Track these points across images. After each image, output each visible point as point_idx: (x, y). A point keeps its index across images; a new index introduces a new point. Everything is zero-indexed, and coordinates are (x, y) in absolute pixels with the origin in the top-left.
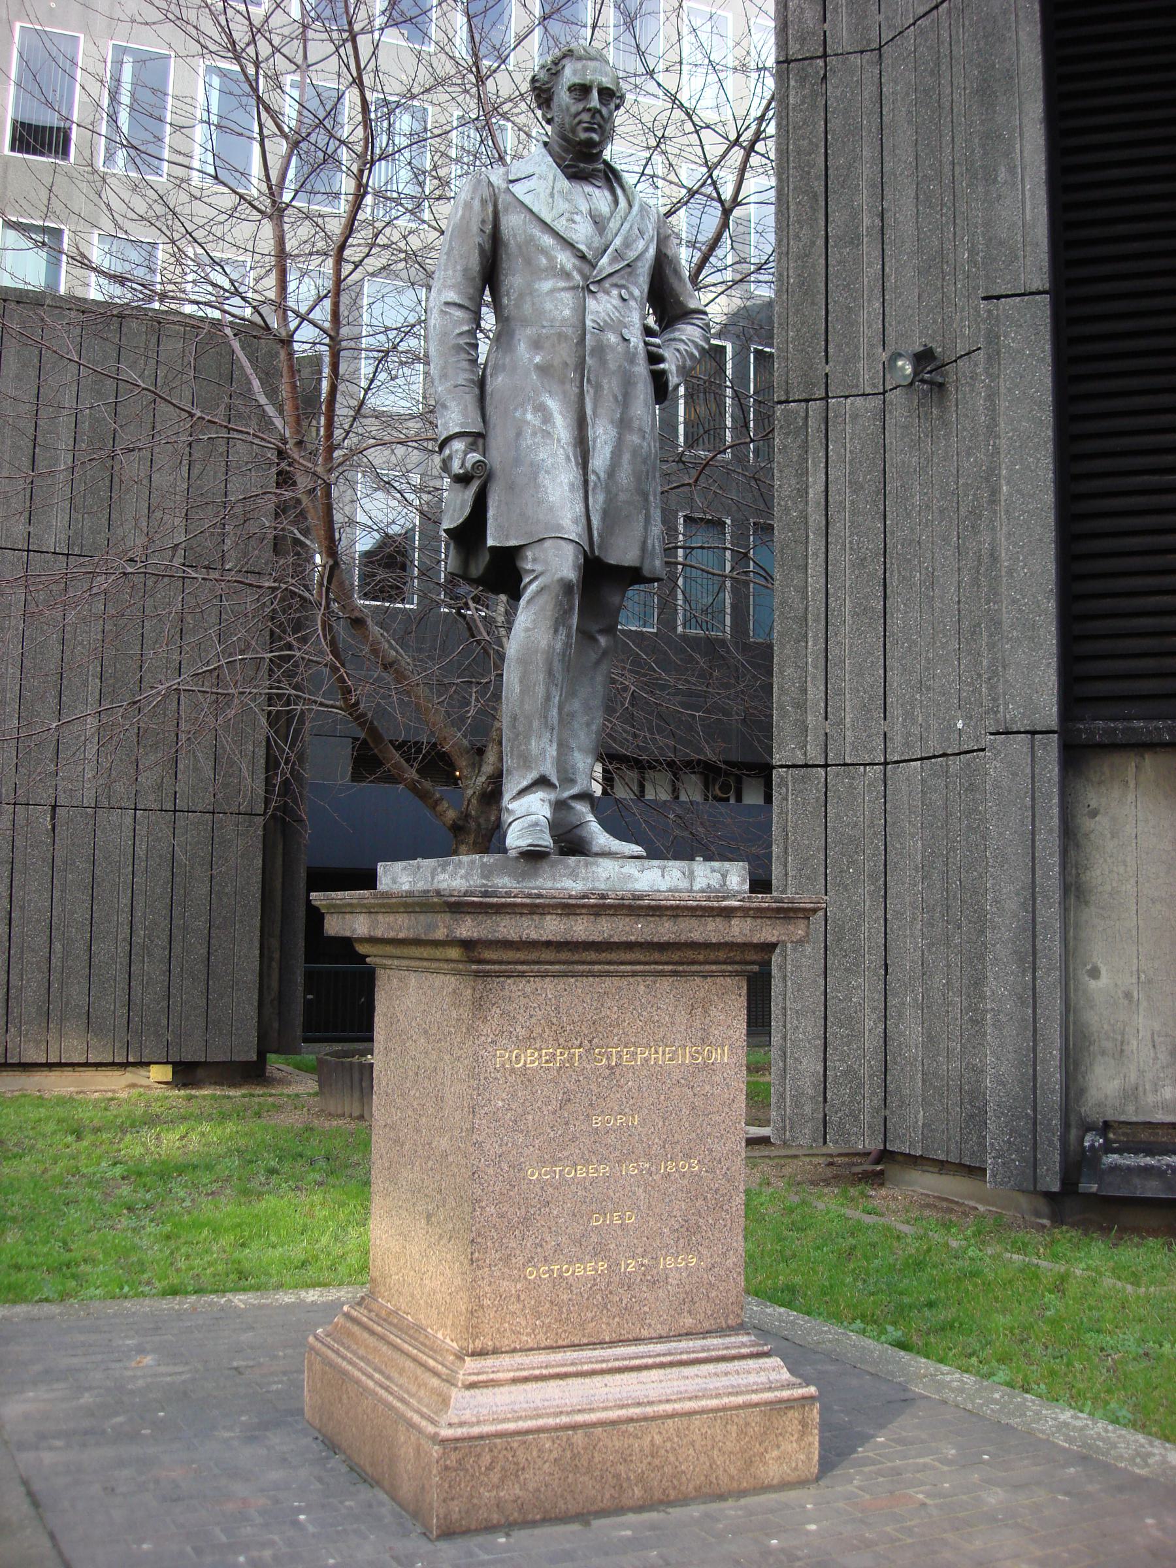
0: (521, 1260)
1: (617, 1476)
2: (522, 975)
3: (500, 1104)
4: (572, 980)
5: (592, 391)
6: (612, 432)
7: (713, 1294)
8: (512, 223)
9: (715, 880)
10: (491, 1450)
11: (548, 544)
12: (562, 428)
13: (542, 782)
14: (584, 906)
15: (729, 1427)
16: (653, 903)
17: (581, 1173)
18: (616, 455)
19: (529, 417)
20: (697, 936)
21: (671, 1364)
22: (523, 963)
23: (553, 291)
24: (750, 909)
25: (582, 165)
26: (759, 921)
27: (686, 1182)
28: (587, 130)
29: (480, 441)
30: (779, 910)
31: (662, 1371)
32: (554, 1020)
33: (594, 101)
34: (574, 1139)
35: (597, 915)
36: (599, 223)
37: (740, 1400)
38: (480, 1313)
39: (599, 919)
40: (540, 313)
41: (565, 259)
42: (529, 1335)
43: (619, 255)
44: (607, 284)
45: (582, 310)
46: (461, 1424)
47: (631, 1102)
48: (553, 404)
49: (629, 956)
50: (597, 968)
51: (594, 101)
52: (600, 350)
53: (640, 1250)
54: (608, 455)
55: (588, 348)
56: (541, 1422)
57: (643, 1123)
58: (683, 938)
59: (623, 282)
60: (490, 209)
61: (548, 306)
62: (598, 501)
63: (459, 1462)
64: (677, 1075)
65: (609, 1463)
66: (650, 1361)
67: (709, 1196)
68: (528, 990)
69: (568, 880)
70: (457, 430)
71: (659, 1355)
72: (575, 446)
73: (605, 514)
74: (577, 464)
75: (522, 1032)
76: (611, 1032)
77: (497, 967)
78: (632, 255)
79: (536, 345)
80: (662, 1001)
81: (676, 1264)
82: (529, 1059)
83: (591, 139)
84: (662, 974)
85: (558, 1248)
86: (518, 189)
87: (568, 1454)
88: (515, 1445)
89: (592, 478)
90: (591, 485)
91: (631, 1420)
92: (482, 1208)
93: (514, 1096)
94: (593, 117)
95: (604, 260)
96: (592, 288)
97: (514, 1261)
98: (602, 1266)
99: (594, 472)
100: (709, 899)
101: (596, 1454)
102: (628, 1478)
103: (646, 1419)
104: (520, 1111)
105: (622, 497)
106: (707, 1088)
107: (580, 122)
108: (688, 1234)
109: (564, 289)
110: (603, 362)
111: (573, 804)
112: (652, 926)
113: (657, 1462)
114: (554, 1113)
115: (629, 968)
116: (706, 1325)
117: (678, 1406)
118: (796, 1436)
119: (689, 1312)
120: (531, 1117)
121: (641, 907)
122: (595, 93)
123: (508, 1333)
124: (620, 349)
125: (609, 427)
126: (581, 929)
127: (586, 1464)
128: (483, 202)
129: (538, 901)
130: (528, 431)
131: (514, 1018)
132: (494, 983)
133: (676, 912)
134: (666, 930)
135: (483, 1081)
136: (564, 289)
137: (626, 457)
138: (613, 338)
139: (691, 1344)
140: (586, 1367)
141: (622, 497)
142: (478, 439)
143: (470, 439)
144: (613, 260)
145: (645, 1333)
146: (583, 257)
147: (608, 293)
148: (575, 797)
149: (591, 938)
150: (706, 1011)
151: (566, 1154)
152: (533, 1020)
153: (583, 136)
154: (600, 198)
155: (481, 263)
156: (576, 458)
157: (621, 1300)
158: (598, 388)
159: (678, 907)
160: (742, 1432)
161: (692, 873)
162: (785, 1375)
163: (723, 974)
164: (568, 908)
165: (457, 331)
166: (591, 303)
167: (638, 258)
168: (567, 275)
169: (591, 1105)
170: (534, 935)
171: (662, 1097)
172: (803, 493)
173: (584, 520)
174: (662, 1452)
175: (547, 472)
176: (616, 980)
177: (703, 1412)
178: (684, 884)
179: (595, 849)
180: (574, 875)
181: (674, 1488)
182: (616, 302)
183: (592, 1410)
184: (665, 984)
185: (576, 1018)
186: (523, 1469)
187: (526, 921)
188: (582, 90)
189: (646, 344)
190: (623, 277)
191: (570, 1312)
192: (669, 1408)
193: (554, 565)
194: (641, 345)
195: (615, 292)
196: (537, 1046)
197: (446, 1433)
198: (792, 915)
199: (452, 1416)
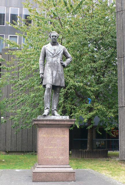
6: (56, 72)
8: (46, 51)
12: (50, 72)
13: (47, 108)
20: (61, 123)
21: (59, 168)
33: (54, 37)
36: (55, 50)
37: (66, 171)
40: (49, 60)
41: (51, 54)
45: (52, 60)
48: (49, 70)
49: (55, 126)
51: (54, 37)
52: (54, 64)
62: (54, 79)
69: (52, 117)
73: (55, 80)
78: (58, 53)
79: (48, 63)
80: (59, 130)
81: (61, 158)
82: (44, 136)
95: (55, 54)
105: (57, 79)
108: (62, 154)
110: (55, 65)
126: (48, 123)
134: (57, 123)
138: (56, 62)
141: (57, 79)
142: (43, 74)
144: (56, 54)
154: (55, 47)
158: (54, 68)
164: (47, 120)
166: (53, 59)
167: (59, 53)
172: (121, 70)
180: (49, 117)
182: (56, 58)
184: (59, 129)
187: (42, 122)
188: (53, 36)
193: (48, 86)
194: (60, 62)
197: (33, 171)
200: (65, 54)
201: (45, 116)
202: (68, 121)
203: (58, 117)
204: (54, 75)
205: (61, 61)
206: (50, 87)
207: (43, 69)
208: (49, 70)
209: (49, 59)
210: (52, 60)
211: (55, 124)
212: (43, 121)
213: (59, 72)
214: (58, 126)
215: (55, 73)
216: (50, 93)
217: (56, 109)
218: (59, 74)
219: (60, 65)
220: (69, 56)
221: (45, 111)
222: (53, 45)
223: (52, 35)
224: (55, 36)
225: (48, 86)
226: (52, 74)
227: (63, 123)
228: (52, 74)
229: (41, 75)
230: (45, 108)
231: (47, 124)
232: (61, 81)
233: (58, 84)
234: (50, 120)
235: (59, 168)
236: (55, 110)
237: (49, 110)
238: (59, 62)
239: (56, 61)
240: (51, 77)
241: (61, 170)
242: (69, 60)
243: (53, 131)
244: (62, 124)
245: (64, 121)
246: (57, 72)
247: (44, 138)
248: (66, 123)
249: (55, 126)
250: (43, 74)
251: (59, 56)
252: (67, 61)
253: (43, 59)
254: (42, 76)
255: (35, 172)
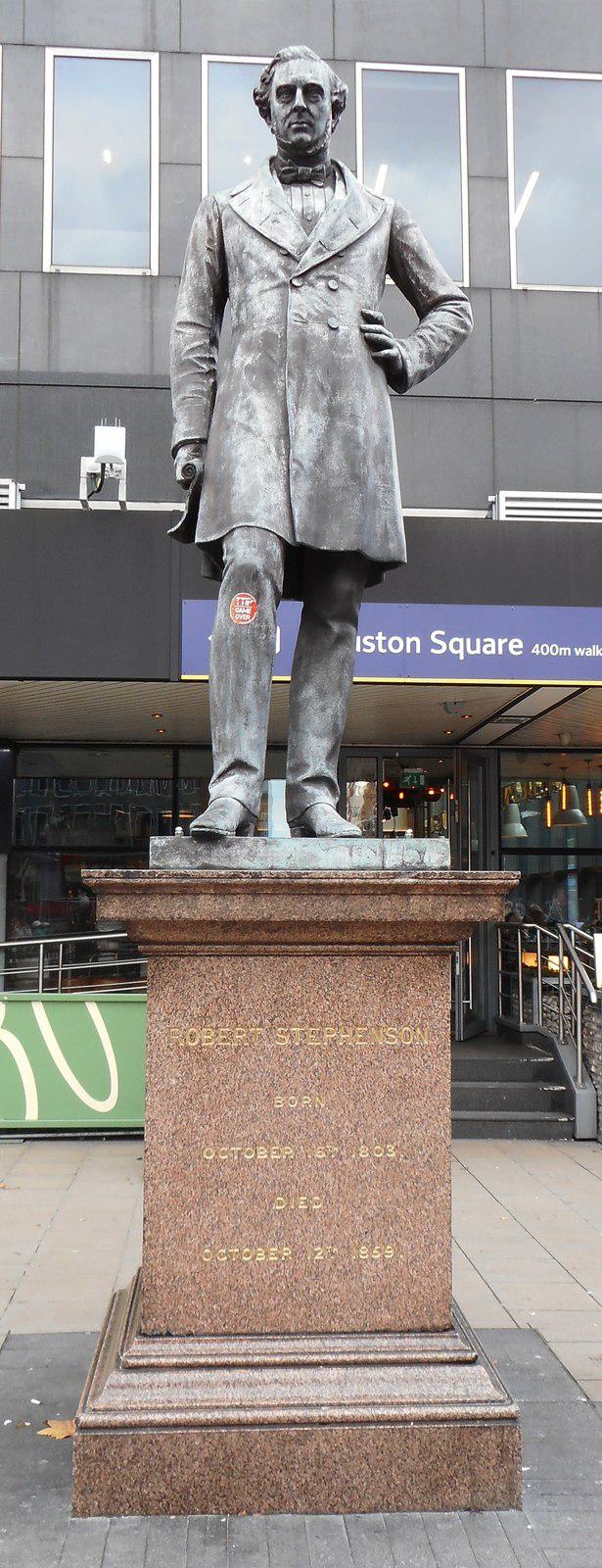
0: (195, 1241)
1: (276, 1484)
2: (194, 954)
3: (174, 1082)
4: (251, 959)
5: (294, 383)
6: (321, 422)
7: (415, 1290)
9: (411, 858)
10: (134, 1442)
11: (236, 533)
12: (265, 421)
13: (239, 765)
14: (236, 885)
15: (409, 1442)
16: (312, 881)
17: (262, 1155)
18: (326, 439)
19: (236, 416)
21: (356, 1364)
22: (192, 943)
23: (262, 292)
24: (428, 886)
25: (300, 169)
26: (443, 898)
27: (381, 1168)
28: (297, 130)
29: (203, 446)
30: (462, 886)
31: (342, 1371)
32: (232, 999)
33: (299, 100)
34: (254, 1119)
35: (255, 894)
36: (308, 222)
37: (424, 1412)
38: (153, 1294)
39: (257, 899)
41: (272, 259)
42: (204, 1319)
43: (323, 247)
44: (312, 277)
45: (284, 303)
46: (106, 1411)
47: (318, 1083)
49: (305, 937)
50: (272, 948)
51: (299, 100)
52: (303, 342)
53: (329, 1238)
54: (314, 443)
55: (289, 341)
56: (190, 1416)
57: (331, 1105)
58: (353, 917)
59: (332, 273)
60: (215, 225)
61: (259, 306)
62: (302, 489)
63: (99, 1451)
64: (369, 1056)
65: (268, 1469)
66: (331, 1358)
67: (408, 1184)
68: (203, 968)
70: (182, 438)
71: (342, 1353)
72: (278, 438)
74: (279, 455)
75: (197, 1011)
76: (295, 1011)
77: (165, 948)
78: (338, 245)
79: (249, 348)
80: (354, 980)
82: (206, 1037)
83: (301, 140)
84: (346, 954)
85: (237, 1231)
86: (235, 203)
87: (221, 1454)
88: (161, 1439)
89: (294, 466)
90: (292, 473)
91: (293, 1423)
92: (155, 1187)
93: (189, 1074)
94: (300, 116)
95: (308, 254)
96: (295, 282)
97: (189, 1241)
98: (287, 1251)
99: (295, 461)
100: (377, 877)
101: (252, 1458)
102: (290, 1488)
103: (310, 1423)
104: (195, 1090)
105: (334, 483)
106: (405, 1070)
107: (290, 125)
109: (272, 288)
111: (309, 789)
112: (318, 904)
113: (323, 1473)
114: (232, 1093)
115: (309, 948)
116: (408, 1323)
117: (348, 1413)
118: (494, 1461)
119: (387, 1307)
120: (207, 1096)
121: (301, 886)
122: (299, 92)
123: (183, 1316)
124: (326, 338)
125: (314, 416)
126: (237, 908)
127: (241, 1468)
128: (209, 222)
129: (184, 881)
130: (235, 428)
131: (189, 996)
132: (167, 964)
133: (344, 890)
134: (332, 909)
135: (155, 1059)
136: (272, 288)
137: (336, 445)
138: (318, 329)
139: (385, 1342)
140: (257, 1359)
141: (334, 483)
142: (199, 445)
143: (193, 446)
144: (319, 252)
145: (336, 1326)
146: (288, 255)
147: (312, 285)
148: (308, 780)
149: (249, 917)
150: (402, 992)
151: (245, 1134)
152: (209, 999)
153: (294, 138)
154: (314, 198)
155: (212, 282)
156: (278, 450)
157: (308, 1289)
158: (302, 379)
159: (342, 886)
160: (424, 1452)
161: (383, 852)
162: (489, 1391)
163: (418, 953)
164: (223, 889)
165: (188, 348)
166: (294, 297)
167: (349, 248)
168: (273, 276)
169: (272, 1085)
170: (186, 915)
171: (353, 1079)
173: (284, 509)
174: (329, 1462)
175: (244, 465)
176: (299, 960)
177: (379, 1421)
178: (376, 862)
179: (318, 830)
180: (252, 855)
181: (345, 1505)
182: (324, 293)
183: (252, 1407)
184: (353, 964)
185: (256, 997)
186: (170, 1466)
187: (178, 902)
188: (287, 92)
189: (362, 331)
190: (332, 268)
191: (250, 1298)
192: (337, 1413)
195: (321, 284)
196: (214, 1024)
197: (86, 1418)
198: (480, 891)
199: (101, 1402)
200: (404, 263)
201: (210, 838)
202: (441, 891)
203: (345, 847)
204: (305, 447)
205: (368, 319)
206: (258, 562)
207: (205, 401)
208: (259, 400)
209: (258, 301)
210: (284, 303)
211: (316, 924)
212: (186, 889)
213: (354, 417)
214: (336, 936)
215: (307, 425)
216: (261, 613)
217: (332, 774)
218: (350, 441)
219: (358, 352)
220: (442, 292)
221: (210, 791)
222: (290, 179)
223: (279, 80)
224: (312, 91)
225: (241, 551)
226: (285, 435)
227: (385, 909)
228: (285, 435)
229: (183, 453)
230: (220, 766)
231: (229, 925)
232: (370, 503)
233: (337, 539)
234: (257, 887)
235: (356, 1364)
236: (318, 780)
237: (253, 778)
238: (350, 329)
239: (323, 318)
240: (273, 463)
241: (373, 1392)
242: (440, 318)
243: (295, 987)
244: (379, 924)
245: (404, 891)
246: (331, 427)
247: (202, 1056)
248: (418, 908)
249: (305, 937)
250: (199, 445)
251: (341, 277)
252: (426, 333)
253: (203, 316)
254: (195, 461)
255: (101, 1418)
